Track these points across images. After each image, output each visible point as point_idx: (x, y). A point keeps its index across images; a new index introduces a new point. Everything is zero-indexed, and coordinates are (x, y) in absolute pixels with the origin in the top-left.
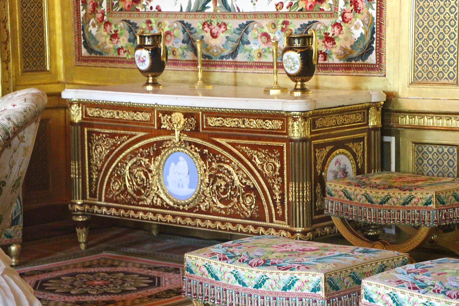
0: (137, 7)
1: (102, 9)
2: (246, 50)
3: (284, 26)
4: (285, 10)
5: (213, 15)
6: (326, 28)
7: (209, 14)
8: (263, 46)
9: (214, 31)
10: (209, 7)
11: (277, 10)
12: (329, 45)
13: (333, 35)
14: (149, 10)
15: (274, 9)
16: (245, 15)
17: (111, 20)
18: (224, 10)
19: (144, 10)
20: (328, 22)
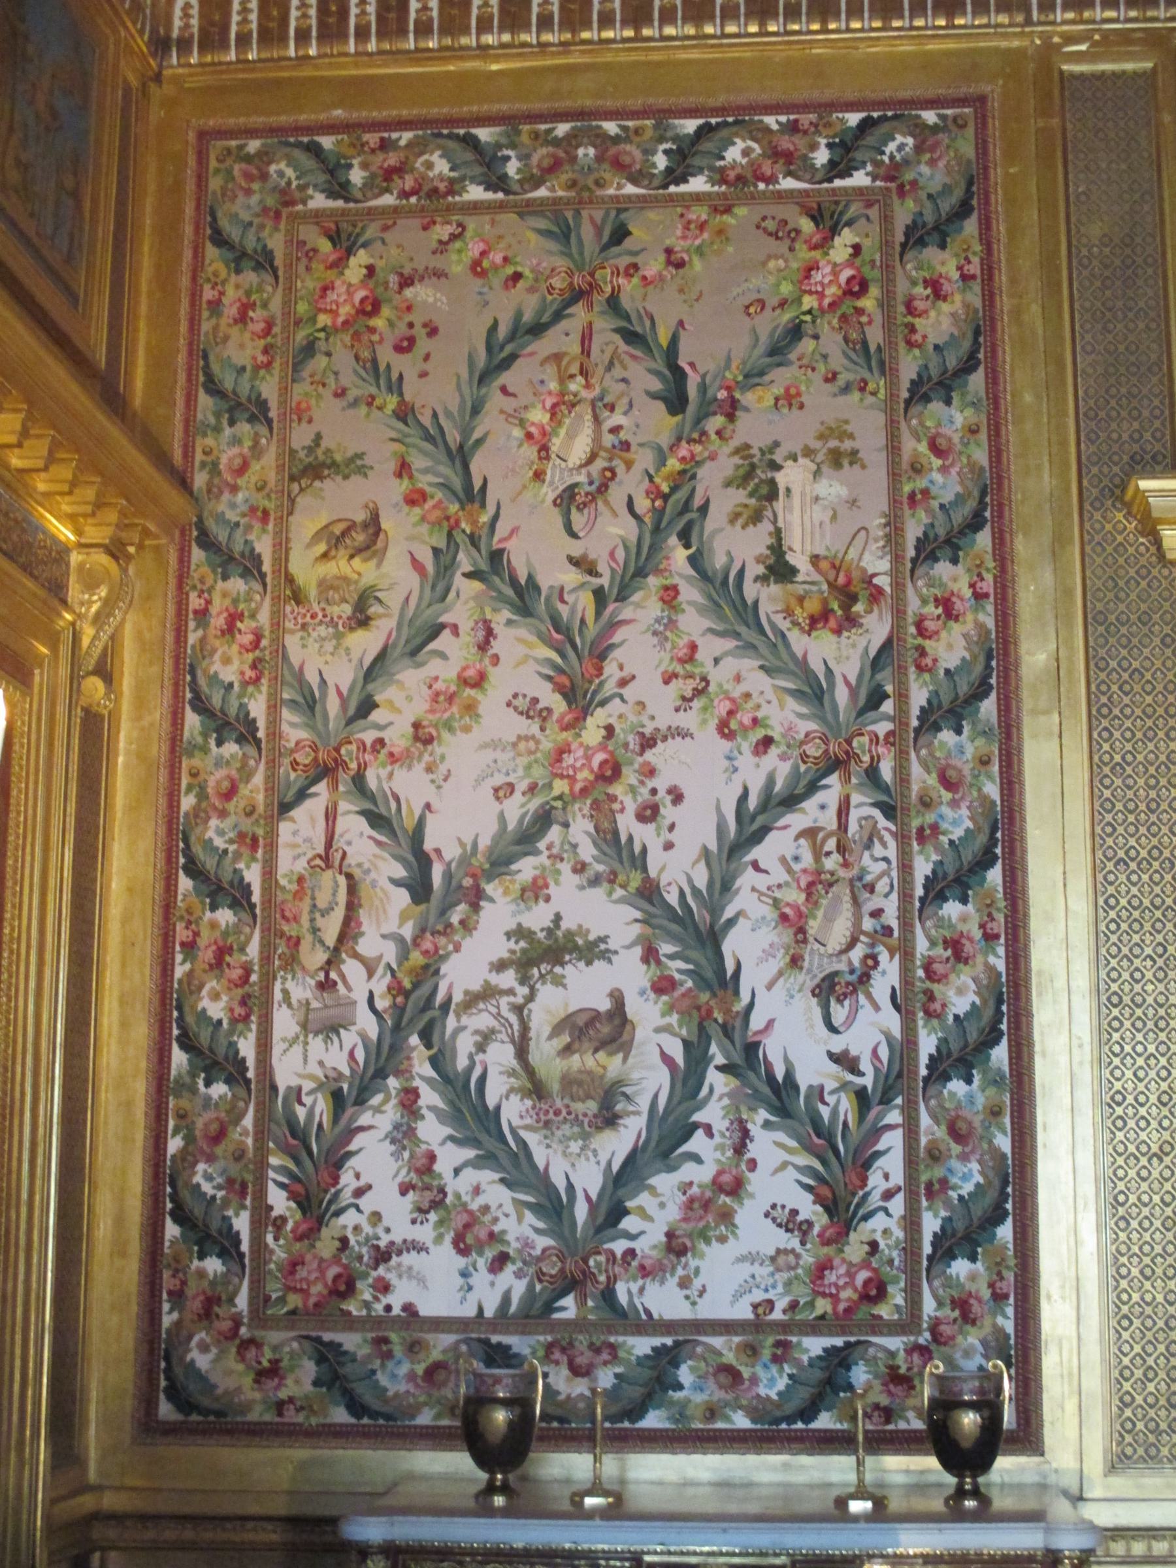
0: (344, 1307)
1: (234, 1310)
2: (672, 1403)
3: (779, 1352)
4: (777, 1315)
5: (577, 1325)
6: (892, 1354)
7: (567, 1323)
8: (720, 1395)
9: (581, 1360)
10: (563, 1309)
11: (757, 1315)
12: (898, 1390)
13: (909, 1369)
14: (382, 1313)
15: (749, 1315)
16: (668, 1327)
17: (259, 1334)
18: (607, 1314)
19: (364, 1313)
20: (895, 1343)
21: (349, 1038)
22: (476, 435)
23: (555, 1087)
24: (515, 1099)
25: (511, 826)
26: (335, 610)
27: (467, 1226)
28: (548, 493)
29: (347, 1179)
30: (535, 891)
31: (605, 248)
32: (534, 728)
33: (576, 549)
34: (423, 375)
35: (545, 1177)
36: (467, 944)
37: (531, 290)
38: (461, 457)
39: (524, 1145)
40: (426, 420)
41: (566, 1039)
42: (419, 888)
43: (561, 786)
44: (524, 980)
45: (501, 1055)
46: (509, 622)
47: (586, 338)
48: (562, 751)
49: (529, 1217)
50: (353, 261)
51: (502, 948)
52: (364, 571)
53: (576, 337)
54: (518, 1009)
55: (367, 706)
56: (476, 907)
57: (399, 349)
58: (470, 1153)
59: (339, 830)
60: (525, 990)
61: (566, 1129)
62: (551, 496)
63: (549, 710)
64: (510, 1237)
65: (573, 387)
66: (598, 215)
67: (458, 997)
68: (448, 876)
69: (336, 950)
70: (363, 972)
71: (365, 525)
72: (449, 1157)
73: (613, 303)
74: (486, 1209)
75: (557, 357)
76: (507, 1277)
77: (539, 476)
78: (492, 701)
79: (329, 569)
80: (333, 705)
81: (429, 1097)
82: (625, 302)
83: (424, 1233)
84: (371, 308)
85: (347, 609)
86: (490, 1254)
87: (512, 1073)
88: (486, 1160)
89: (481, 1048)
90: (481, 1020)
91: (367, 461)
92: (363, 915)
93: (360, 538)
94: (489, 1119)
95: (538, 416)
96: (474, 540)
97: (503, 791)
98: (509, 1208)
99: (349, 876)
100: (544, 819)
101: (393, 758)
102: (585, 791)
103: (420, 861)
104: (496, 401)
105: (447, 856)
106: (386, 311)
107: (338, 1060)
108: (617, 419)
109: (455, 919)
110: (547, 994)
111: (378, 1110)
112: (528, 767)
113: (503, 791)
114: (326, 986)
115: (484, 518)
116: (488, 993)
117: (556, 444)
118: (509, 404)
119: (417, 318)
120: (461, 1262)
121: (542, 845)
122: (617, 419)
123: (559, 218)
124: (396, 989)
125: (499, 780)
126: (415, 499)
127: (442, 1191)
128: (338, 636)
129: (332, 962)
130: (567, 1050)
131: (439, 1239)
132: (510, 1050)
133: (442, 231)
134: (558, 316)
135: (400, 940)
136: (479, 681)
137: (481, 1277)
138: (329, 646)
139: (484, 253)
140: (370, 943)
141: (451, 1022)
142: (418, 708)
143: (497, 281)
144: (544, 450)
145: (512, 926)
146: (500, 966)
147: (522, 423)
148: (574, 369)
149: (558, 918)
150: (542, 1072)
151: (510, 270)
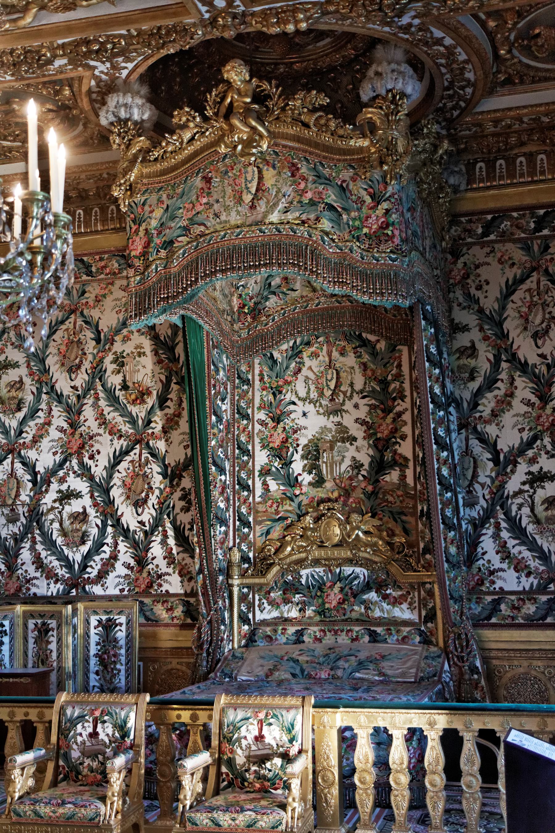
21: (478, 508)
22: (505, 316)
23: (543, 521)
24: (531, 525)
25: (525, 440)
26: (463, 375)
27: (518, 563)
28: (529, 334)
29: (479, 549)
30: (533, 461)
31: (542, 253)
32: (530, 410)
33: (540, 351)
34: (486, 297)
35: (541, 548)
36: (513, 477)
37: (519, 268)
38: (500, 324)
39: (534, 539)
40: (488, 313)
41: (546, 505)
42: (496, 460)
43: (539, 428)
44: (532, 487)
45: (526, 510)
46: (519, 376)
47: (538, 283)
48: (539, 417)
49: (537, 561)
50: (459, 261)
51: (524, 478)
52: (472, 362)
53: (535, 283)
54: (530, 497)
55: (476, 405)
56: (515, 466)
57: (477, 289)
58: (517, 542)
59: (470, 443)
60: (532, 491)
61: (548, 534)
62: (530, 335)
63: (534, 403)
64: (532, 566)
65: (535, 299)
66: (539, 242)
67: (511, 493)
68: (505, 457)
69: (471, 481)
70: (481, 488)
71: (471, 347)
72: (511, 543)
73: (546, 271)
74: (523, 558)
75: (529, 290)
76: (531, 579)
77: (525, 329)
78: (516, 402)
79: (461, 362)
80: (465, 405)
81: (503, 524)
82: (551, 271)
83: (505, 566)
84: (466, 276)
85: (467, 375)
86: (525, 572)
87: (529, 517)
88: (522, 543)
89: (519, 509)
90: (519, 500)
91: (470, 327)
92: (479, 470)
93: (470, 352)
94: (523, 531)
95: (524, 309)
96: (506, 350)
97: (521, 430)
98: (530, 558)
99: (474, 458)
100: (535, 438)
101: (486, 422)
102: (548, 429)
103: (496, 453)
104: (510, 305)
105: (505, 451)
106: (472, 277)
107: (475, 514)
108: (550, 309)
109: (508, 470)
110: (540, 492)
111: (488, 528)
112: (529, 422)
113: (521, 430)
114: (469, 492)
115: (509, 343)
116: (521, 492)
117: (530, 318)
118: (514, 306)
119: (483, 278)
120: (517, 574)
121: (535, 446)
122: (550, 309)
123: (526, 244)
124: (491, 492)
125: (520, 427)
126: (486, 338)
127: (509, 553)
128: (465, 383)
129: (471, 484)
130: (547, 509)
131: (509, 568)
132: (528, 509)
133: (488, 250)
134: (528, 277)
135: (490, 477)
136: (512, 395)
137: (523, 579)
138: (462, 387)
139: (502, 256)
140: (482, 479)
141: (510, 501)
142: (493, 404)
143: (507, 266)
144: (527, 320)
145: (527, 471)
146: (524, 483)
147: (519, 312)
148: (535, 293)
149: (541, 468)
150: (539, 516)
151: (511, 262)
